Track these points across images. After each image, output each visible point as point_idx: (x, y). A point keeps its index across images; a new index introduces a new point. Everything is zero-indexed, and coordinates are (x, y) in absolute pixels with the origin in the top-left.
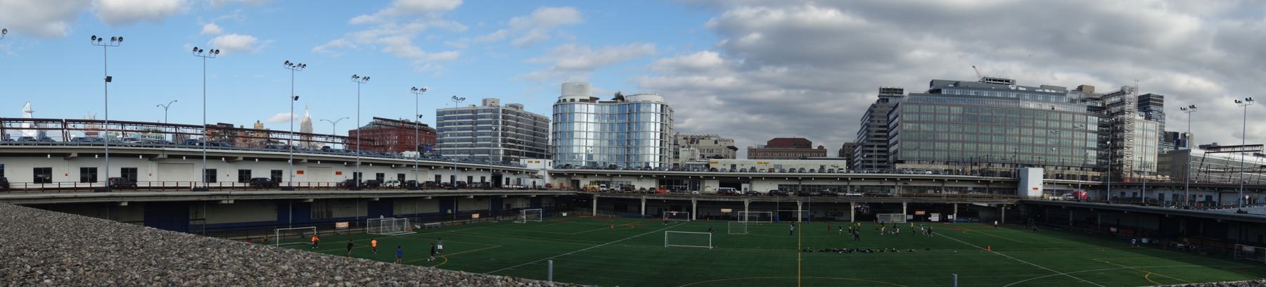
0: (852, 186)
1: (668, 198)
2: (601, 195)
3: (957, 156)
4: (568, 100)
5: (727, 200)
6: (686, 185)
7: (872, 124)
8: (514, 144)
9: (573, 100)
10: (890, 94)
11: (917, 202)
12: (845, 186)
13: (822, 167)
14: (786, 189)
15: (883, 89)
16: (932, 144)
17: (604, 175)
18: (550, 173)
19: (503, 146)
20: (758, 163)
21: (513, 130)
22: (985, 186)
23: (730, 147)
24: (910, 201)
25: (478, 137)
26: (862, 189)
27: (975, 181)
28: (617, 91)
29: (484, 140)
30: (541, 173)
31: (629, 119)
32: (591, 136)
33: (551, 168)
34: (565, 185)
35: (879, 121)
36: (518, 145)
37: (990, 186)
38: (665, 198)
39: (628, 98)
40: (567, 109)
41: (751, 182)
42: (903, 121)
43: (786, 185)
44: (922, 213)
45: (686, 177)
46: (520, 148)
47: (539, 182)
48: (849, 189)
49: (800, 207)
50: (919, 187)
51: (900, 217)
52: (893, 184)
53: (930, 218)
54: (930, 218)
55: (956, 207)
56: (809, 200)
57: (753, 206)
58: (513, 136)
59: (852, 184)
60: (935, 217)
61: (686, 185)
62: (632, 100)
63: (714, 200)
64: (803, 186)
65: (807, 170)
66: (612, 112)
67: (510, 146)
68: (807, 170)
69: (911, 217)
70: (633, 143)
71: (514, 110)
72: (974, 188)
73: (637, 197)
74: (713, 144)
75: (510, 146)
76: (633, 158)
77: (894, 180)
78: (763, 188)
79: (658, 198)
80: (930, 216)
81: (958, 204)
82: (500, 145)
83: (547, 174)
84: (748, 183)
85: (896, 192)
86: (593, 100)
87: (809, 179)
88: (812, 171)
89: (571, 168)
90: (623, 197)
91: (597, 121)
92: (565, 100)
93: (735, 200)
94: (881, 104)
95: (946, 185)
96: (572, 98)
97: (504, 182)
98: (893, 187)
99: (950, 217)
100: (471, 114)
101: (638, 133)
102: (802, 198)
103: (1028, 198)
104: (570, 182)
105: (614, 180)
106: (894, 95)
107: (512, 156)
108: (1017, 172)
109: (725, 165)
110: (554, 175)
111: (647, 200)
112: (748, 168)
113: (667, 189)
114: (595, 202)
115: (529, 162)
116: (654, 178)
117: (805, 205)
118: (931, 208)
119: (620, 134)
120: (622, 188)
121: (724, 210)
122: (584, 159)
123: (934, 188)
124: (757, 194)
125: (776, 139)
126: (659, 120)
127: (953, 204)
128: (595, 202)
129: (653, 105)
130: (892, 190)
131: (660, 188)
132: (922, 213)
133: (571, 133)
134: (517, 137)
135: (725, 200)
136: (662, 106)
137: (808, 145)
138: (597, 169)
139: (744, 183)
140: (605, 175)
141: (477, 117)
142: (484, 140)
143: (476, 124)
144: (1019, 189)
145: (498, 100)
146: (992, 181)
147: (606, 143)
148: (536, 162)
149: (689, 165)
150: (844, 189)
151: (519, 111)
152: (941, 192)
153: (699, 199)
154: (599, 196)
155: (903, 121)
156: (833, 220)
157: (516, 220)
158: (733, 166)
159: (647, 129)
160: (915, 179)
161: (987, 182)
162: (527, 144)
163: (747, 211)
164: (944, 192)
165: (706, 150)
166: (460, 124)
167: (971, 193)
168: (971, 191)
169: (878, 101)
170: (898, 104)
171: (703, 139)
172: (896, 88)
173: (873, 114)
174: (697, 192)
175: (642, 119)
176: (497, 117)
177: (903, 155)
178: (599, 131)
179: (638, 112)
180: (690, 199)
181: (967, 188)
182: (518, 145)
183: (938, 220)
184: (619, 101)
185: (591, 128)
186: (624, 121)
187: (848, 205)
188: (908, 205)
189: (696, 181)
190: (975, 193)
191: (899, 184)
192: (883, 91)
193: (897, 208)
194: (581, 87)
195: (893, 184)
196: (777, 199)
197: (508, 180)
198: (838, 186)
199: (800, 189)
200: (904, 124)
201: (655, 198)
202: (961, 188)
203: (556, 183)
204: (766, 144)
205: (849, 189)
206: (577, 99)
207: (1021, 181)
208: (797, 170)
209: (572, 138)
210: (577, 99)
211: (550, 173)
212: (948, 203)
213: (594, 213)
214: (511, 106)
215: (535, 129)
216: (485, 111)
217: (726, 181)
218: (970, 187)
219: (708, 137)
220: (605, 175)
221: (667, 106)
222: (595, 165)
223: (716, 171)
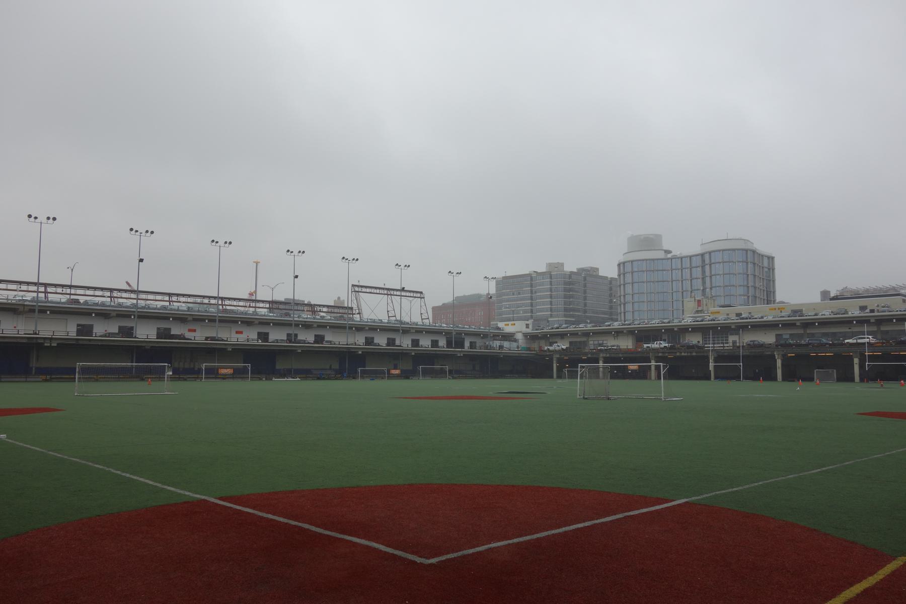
18: (525, 335)
33: (529, 330)
84: (738, 334)
109: (728, 314)
115: (506, 325)
154: (558, 356)
158: (738, 315)
211: (525, 335)
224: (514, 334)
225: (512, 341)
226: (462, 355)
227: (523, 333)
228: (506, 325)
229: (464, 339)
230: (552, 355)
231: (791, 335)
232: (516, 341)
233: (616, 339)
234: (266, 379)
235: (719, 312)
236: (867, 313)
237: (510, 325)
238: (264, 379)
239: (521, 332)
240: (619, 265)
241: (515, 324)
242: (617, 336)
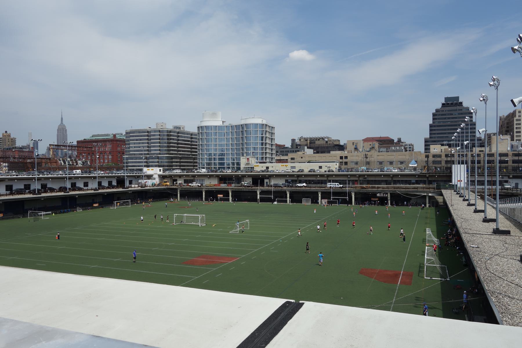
6: (234, 180)
8: (176, 152)
18: (159, 176)
25: (152, 148)
29: (155, 150)
33: (161, 173)
41: (269, 178)
67: (172, 154)
75: (172, 154)
84: (268, 179)
97: (127, 184)
100: (147, 134)
115: (148, 170)
141: (151, 136)
142: (155, 150)
143: (150, 140)
148: (151, 170)
166: (141, 140)
181: (411, 181)
189: (239, 179)
198: (321, 180)
211: (159, 176)
216: (155, 131)
224: (153, 175)
225: (153, 179)
226: (131, 192)
227: (158, 175)
228: (148, 170)
231: (292, 180)
232: (154, 179)
234: (23, 217)
235: (258, 166)
236: (323, 170)
237: (150, 170)
238: (21, 217)
239: (157, 174)
241: (153, 170)
242: (210, 177)
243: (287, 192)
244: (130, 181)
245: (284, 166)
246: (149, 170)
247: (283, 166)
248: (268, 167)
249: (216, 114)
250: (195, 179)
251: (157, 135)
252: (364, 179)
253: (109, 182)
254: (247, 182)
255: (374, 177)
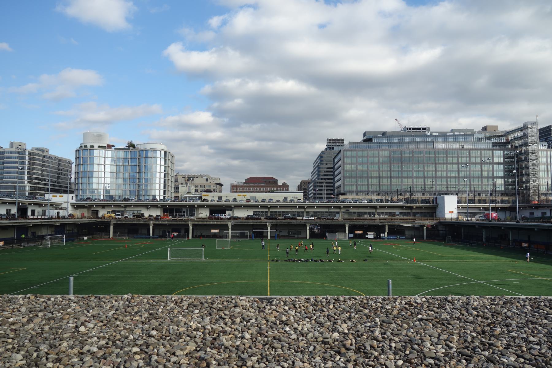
0: (308, 212)
1: (170, 223)
2: (117, 222)
3: (386, 189)
4: (89, 146)
5: (215, 223)
6: (184, 212)
7: (322, 166)
8: (40, 182)
9: (92, 147)
10: (335, 144)
11: (356, 224)
12: (303, 213)
13: (286, 198)
14: (259, 215)
15: (330, 140)
16: (366, 180)
17: (119, 206)
18: (73, 205)
19: (29, 183)
20: (238, 195)
21: (38, 170)
22: (410, 211)
23: (217, 184)
24: (351, 223)
26: (315, 214)
27: (401, 207)
28: (129, 141)
29: (10, 177)
30: (64, 205)
31: (139, 163)
32: (108, 175)
33: (73, 201)
34: (86, 214)
35: (327, 164)
36: (43, 182)
37: (413, 211)
38: (168, 223)
39: (139, 146)
40: (88, 154)
41: (233, 209)
42: (344, 164)
43: (259, 212)
44: (361, 232)
45: (184, 206)
46: (45, 185)
47: (62, 213)
48: (305, 214)
49: (269, 228)
50: (358, 212)
51: (344, 235)
52: (338, 210)
53: (366, 236)
54: (366, 236)
55: (387, 227)
56: (276, 222)
57: (234, 227)
58: (39, 174)
59: (307, 210)
60: (370, 235)
61: (184, 212)
62: (142, 147)
63: (205, 223)
64: (271, 212)
65: (275, 200)
66: (125, 157)
67: (35, 183)
68: (275, 200)
69: (352, 235)
70: (143, 181)
71: (41, 153)
72: (400, 213)
73: (146, 223)
74: (205, 181)
75: (35, 183)
76: (143, 193)
77: (339, 207)
78: (242, 214)
79: (163, 223)
80: (367, 234)
81: (388, 225)
82: (26, 182)
83: (70, 206)
84: (231, 210)
85: (340, 217)
86: (109, 147)
87: (276, 207)
88: (278, 201)
89: (91, 201)
90: (135, 222)
91: (113, 163)
92: (86, 146)
93: (221, 223)
94: (328, 151)
95: (378, 211)
96: (92, 145)
97: (29, 213)
98: (338, 213)
99: (382, 235)
101: (146, 173)
102: (271, 221)
103: (446, 221)
104: (90, 212)
105: (127, 209)
106: (337, 144)
107: (37, 191)
108: (435, 200)
109: (213, 197)
110: (76, 207)
111: (154, 224)
112: (231, 199)
113: (170, 215)
114: (112, 227)
115: (53, 196)
116: (160, 207)
117: (273, 227)
118: (367, 228)
119: (133, 174)
120: (134, 216)
121: (213, 231)
122: (102, 193)
123: (369, 213)
124: (237, 218)
125: (251, 178)
126: (163, 163)
127: (385, 225)
128: (112, 227)
129: (158, 152)
130: (337, 215)
131: (164, 215)
132: (361, 232)
133: (91, 173)
134: (43, 175)
135: (214, 223)
136: (165, 153)
137: (275, 182)
138: (114, 201)
139: (228, 210)
140: (121, 206)
142: (10, 177)
144: (437, 213)
145: (25, 144)
146: (415, 207)
147: (120, 181)
148: (60, 196)
149: (186, 197)
150: (302, 214)
151: (44, 154)
152: (374, 216)
153: (194, 223)
155: (344, 164)
156: (294, 237)
157: (41, 245)
158: (220, 198)
159: (154, 171)
160: (354, 207)
161: (411, 208)
162: (51, 182)
163: (230, 231)
164: (377, 216)
165: (199, 186)
167: (398, 217)
168: (398, 215)
169: (326, 149)
170: (340, 151)
171: (197, 177)
172: (339, 139)
173: (323, 159)
174: (193, 218)
175: (149, 163)
176: (24, 158)
177: (345, 189)
178: (115, 171)
179: (147, 157)
180: (187, 223)
181: (395, 213)
182: (43, 182)
183: (373, 238)
184: (131, 148)
185: (108, 169)
186: (135, 164)
187: (305, 226)
188: (350, 227)
189: (192, 209)
190: (402, 217)
191: (343, 210)
192: (330, 141)
193: (341, 228)
194: (100, 137)
195: (338, 210)
196: (252, 222)
197: (33, 213)
198: (297, 212)
199: (269, 215)
200: (345, 166)
201: (161, 223)
202: (390, 213)
203: (78, 213)
204: (244, 182)
205: (305, 214)
206: (96, 146)
207: (439, 206)
208: (267, 200)
209: (92, 177)
210: (96, 146)
211: (73, 205)
212: (381, 224)
213: (111, 236)
214: (37, 149)
215: (59, 169)
216: (11, 152)
217: (216, 209)
218: (397, 212)
219: (201, 176)
220: (121, 206)
221: (169, 153)
222: (111, 198)
223: (207, 201)
229: (28, 207)
230: (110, 221)
233: (148, 209)
240: (76, 151)
241: (63, 196)
243: (268, 225)
244: (32, 210)
245: (241, 195)
246: (56, 196)
247: (240, 197)
248: (221, 197)
249: (101, 135)
250: (127, 210)
251: (15, 158)
252: (346, 210)
253: (7, 210)
254: (204, 214)
255: (357, 208)
